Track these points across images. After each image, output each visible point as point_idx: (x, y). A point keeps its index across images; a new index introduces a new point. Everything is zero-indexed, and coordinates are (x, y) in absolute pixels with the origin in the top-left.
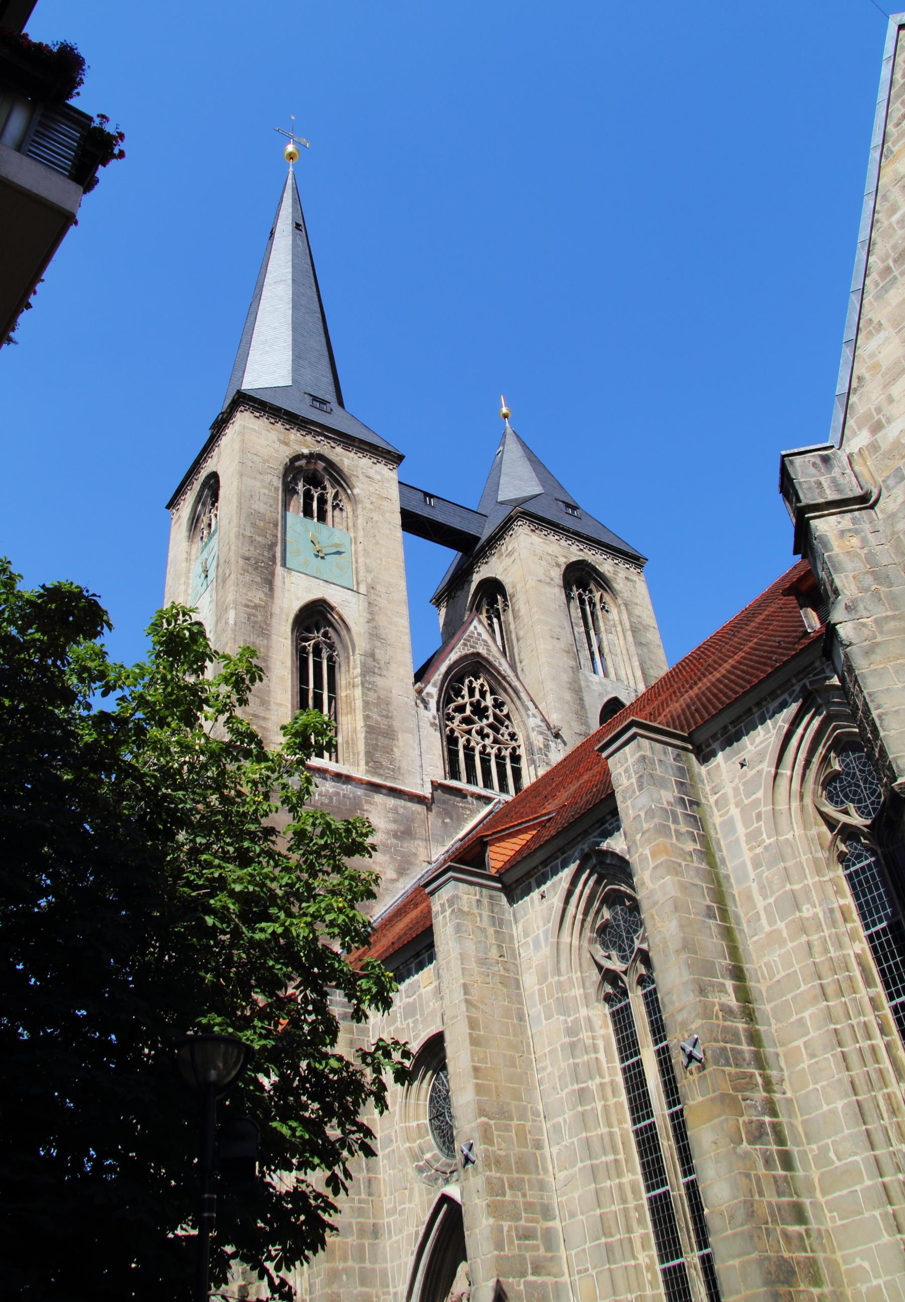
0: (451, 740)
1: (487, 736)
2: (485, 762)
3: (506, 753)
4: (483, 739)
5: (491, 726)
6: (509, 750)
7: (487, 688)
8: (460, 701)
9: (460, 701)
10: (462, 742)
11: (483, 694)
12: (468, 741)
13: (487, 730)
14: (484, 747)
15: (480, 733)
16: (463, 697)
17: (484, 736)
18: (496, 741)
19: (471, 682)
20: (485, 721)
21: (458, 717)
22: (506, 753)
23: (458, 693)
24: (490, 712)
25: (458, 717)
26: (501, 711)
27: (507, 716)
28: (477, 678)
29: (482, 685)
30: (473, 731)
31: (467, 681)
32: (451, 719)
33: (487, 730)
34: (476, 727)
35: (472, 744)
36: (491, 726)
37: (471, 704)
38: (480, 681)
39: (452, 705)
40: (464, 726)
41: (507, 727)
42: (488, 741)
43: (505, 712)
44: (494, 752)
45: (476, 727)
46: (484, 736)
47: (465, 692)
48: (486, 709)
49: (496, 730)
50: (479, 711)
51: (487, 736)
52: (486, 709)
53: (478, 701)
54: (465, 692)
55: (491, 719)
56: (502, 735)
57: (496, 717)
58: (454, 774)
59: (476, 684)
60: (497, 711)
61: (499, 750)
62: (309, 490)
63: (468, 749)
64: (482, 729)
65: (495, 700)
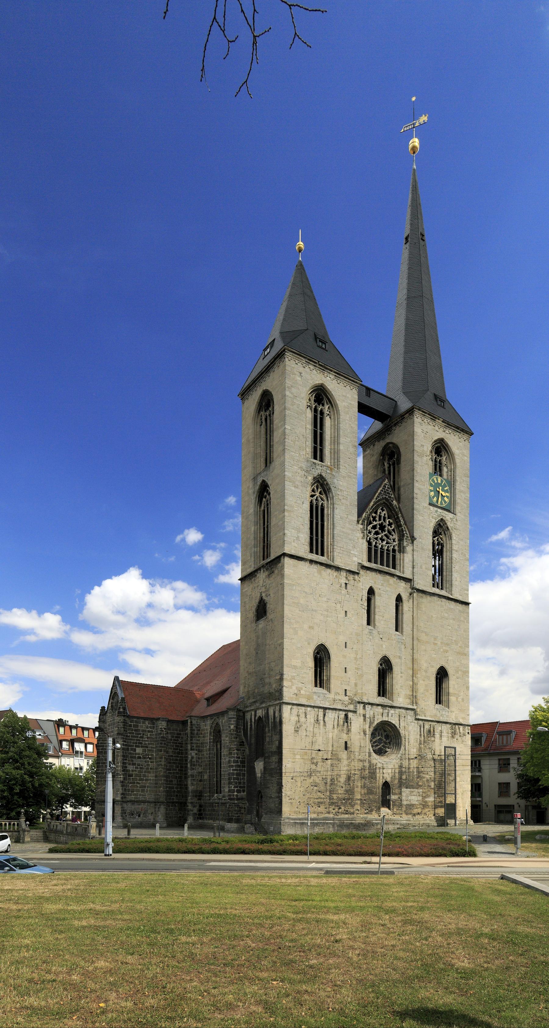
0: (369, 543)
2: (382, 553)
5: (385, 535)
6: (392, 547)
7: (386, 516)
8: (375, 523)
9: (375, 523)
10: (374, 543)
11: (384, 518)
12: (376, 543)
13: (384, 538)
14: (382, 546)
15: (381, 539)
16: (376, 521)
17: (382, 540)
18: (387, 543)
19: (380, 513)
20: (384, 533)
21: (373, 531)
22: (391, 548)
23: (374, 519)
24: (386, 529)
25: (373, 531)
26: (391, 527)
27: (393, 530)
28: (383, 510)
29: (385, 514)
30: (379, 539)
32: (370, 532)
33: (384, 538)
34: (380, 536)
35: (377, 545)
36: (385, 535)
38: (384, 512)
39: (371, 525)
40: (376, 536)
42: (384, 543)
44: (386, 548)
45: (380, 536)
46: (382, 540)
47: (377, 519)
48: (385, 526)
49: (388, 537)
50: (382, 528)
54: (377, 519)
55: (386, 532)
57: (389, 531)
58: (370, 560)
61: (388, 547)
63: (375, 546)
64: (382, 537)
65: (389, 522)
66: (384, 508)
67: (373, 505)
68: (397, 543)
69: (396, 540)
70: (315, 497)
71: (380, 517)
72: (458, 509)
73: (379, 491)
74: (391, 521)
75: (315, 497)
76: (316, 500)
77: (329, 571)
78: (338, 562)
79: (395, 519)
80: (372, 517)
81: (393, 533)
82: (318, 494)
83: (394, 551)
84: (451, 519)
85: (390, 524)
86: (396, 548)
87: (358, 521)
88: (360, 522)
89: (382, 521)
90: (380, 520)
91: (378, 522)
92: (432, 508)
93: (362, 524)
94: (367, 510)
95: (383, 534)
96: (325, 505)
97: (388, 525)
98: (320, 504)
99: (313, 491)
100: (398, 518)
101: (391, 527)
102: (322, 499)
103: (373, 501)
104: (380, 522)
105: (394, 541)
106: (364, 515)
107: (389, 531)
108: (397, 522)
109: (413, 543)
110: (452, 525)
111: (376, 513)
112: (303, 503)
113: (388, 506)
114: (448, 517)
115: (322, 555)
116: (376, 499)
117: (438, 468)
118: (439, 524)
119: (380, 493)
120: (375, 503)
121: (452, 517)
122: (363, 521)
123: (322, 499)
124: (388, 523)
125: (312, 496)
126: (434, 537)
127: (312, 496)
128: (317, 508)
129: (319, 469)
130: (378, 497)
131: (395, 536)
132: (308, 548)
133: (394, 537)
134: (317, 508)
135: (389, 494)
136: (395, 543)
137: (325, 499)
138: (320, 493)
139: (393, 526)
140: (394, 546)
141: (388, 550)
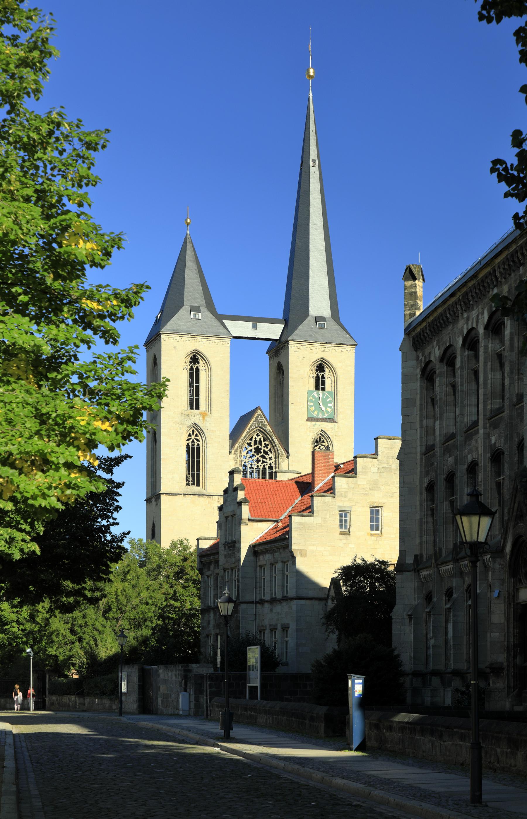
1: (260, 461)
3: (267, 467)
4: (258, 463)
6: (269, 465)
7: (262, 440)
13: (260, 459)
14: (258, 466)
16: (251, 446)
17: (258, 461)
19: (255, 438)
20: (260, 455)
22: (267, 467)
24: (262, 451)
26: (267, 448)
27: (270, 450)
28: (258, 435)
29: (260, 439)
31: (254, 439)
33: (260, 459)
37: (255, 448)
38: (259, 437)
41: (269, 455)
42: (260, 463)
43: (269, 449)
44: (261, 468)
46: (258, 461)
47: (252, 444)
48: (261, 449)
50: (258, 450)
51: (260, 461)
52: (261, 449)
53: (258, 447)
54: (252, 444)
55: (262, 454)
56: (266, 459)
59: (258, 439)
60: (265, 449)
61: (264, 466)
62: (192, 367)
63: (251, 468)
64: (258, 458)
65: (265, 444)
66: (259, 434)
67: (246, 435)
68: (273, 460)
69: (273, 458)
70: (191, 440)
71: (255, 442)
72: (340, 418)
73: (251, 422)
74: (267, 443)
75: (191, 440)
76: (193, 441)
77: (201, 499)
78: (210, 491)
79: (270, 441)
80: (247, 443)
81: (269, 453)
82: (193, 437)
83: (271, 467)
84: (331, 428)
85: (266, 446)
86: (272, 465)
87: (230, 453)
88: (233, 452)
89: (258, 445)
90: (255, 445)
91: (253, 447)
92: (309, 423)
93: (235, 454)
94: (240, 441)
95: (258, 456)
96: (201, 445)
97: (264, 447)
98: (196, 445)
99: (190, 435)
100: (272, 440)
101: (267, 448)
102: (198, 440)
103: (246, 432)
104: (256, 446)
105: (271, 459)
106: (237, 445)
107: (264, 451)
108: (272, 444)
109: (288, 457)
110: (332, 434)
111: (251, 439)
112: (177, 450)
113: (262, 432)
114: (327, 427)
115: (198, 485)
116: (249, 429)
117: (320, 384)
118: (321, 434)
119: (253, 423)
120: (248, 433)
121: (333, 426)
122: (236, 451)
123: (198, 440)
124: (263, 445)
125: (188, 440)
126: (316, 446)
127: (188, 440)
128: (193, 448)
129: (195, 417)
130: (251, 427)
131: (272, 455)
132: (185, 482)
133: (270, 456)
134: (193, 448)
135: (262, 422)
136: (271, 461)
137: (200, 439)
138: (196, 435)
139: (269, 447)
140: (270, 464)
141: (264, 468)
